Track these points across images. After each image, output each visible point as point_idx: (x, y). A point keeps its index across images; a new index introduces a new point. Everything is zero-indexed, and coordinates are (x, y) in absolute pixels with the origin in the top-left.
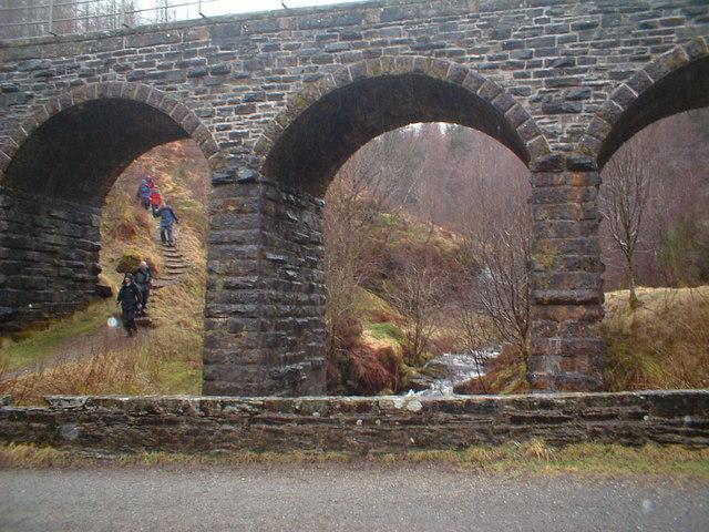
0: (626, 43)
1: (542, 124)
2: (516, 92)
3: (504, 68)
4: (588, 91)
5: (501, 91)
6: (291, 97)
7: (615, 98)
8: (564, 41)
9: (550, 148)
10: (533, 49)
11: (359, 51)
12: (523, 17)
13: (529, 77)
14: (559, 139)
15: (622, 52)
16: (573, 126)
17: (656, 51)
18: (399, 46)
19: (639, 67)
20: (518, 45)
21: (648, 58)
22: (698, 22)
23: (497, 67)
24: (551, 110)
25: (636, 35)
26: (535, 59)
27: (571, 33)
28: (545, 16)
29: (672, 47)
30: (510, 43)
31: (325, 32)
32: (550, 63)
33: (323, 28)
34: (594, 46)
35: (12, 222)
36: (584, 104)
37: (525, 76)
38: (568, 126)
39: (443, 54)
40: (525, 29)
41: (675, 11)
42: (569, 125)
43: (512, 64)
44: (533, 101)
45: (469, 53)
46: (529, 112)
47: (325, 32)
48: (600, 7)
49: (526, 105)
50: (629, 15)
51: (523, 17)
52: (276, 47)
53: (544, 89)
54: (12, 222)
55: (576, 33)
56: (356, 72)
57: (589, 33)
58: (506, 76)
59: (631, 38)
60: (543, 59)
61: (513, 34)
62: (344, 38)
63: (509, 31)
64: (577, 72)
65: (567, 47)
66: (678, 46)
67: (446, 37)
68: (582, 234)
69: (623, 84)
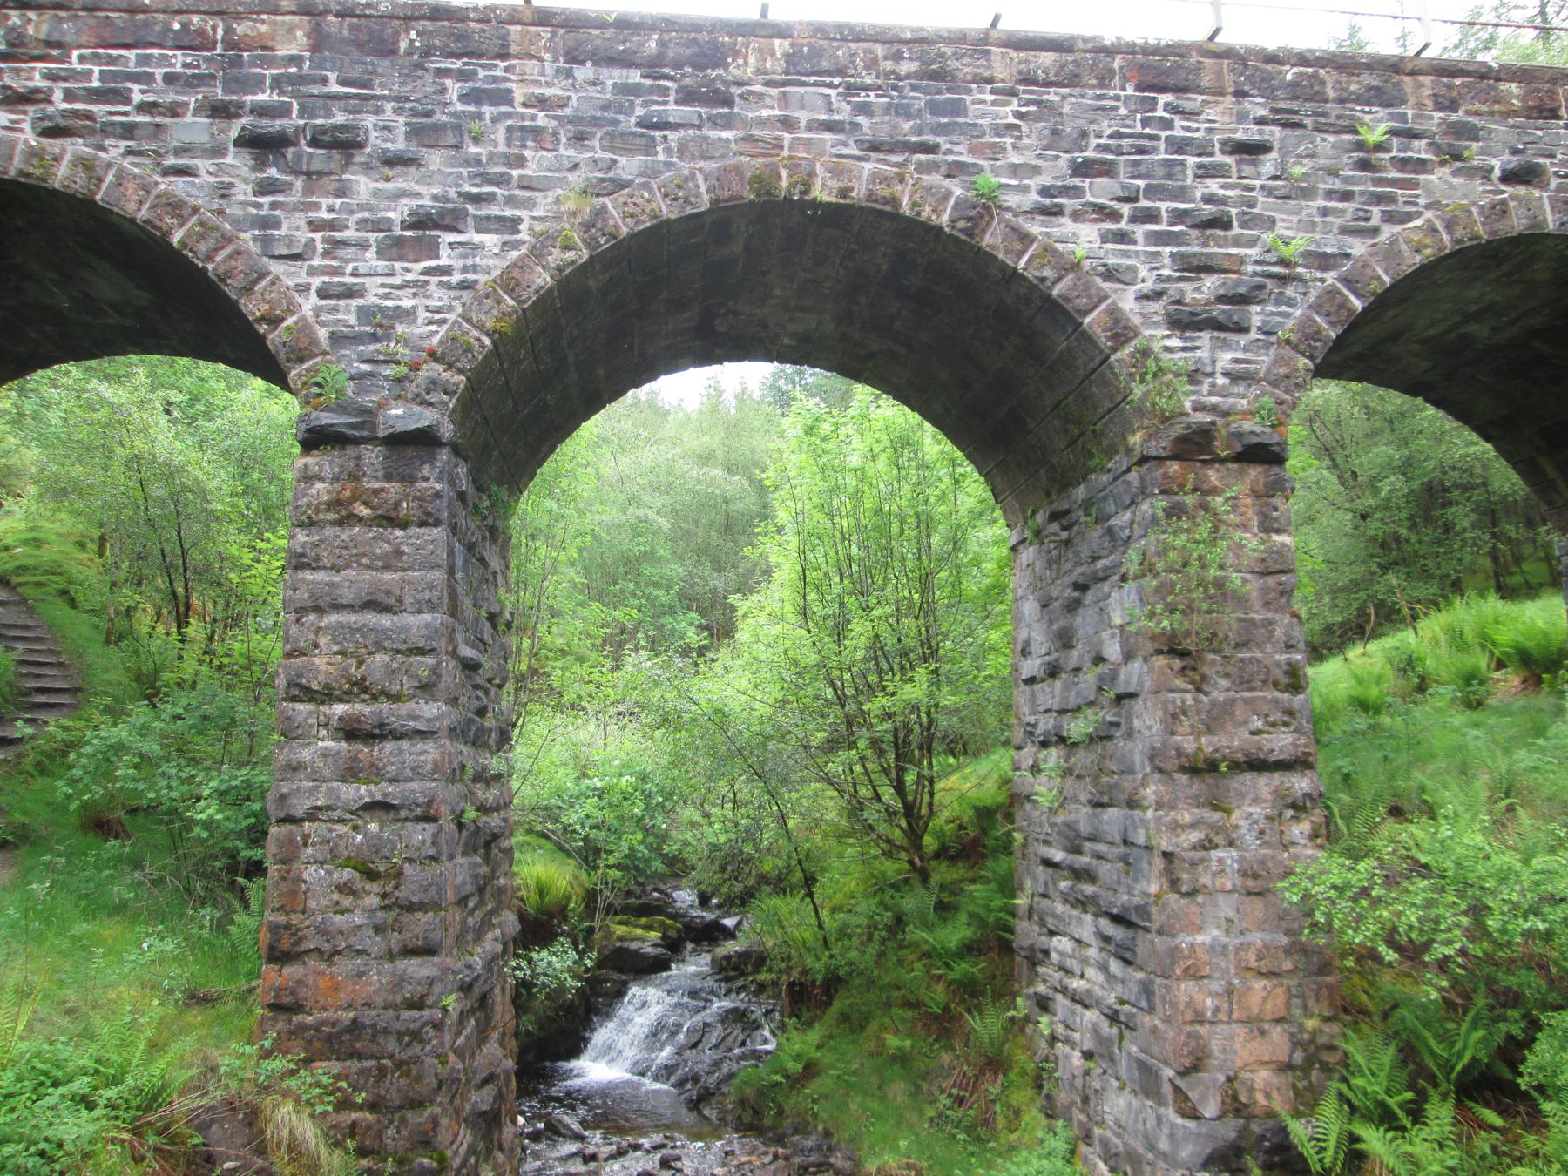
0: (1330, 194)
1: (1168, 349)
2: (1110, 274)
3: (1076, 216)
4: (1261, 287)
5: (1076, 266)
6: (538, 227)
7: (1316, 307)
8: (1205, 172)
9: (1188, 405)
10: (1141, 183)
11: (725, 134)
12: (1116, 108)
13: (1134, 242)
14: (1205, 388)
15: (1325, 212)
16: (1236, 361)
17: (1389, 218)
18: (827, 136)
19: (1358, 247)
20: (1107, 170)
21: (1375, 231)
22: (1456, 173)
23: (1056, 211)
24: (1185, 322)
25: (1347, 180)
26: (1144, 203)
27: (1219, 158)
28: (1160, 113)
29: (1419, 214)
30: (1088, 163)
31: (635, 76)
32: (1178, 216)
33: (631, 65)
34: (1269, 191)
35: (498, 354)
36: (1256, 314)
37: (1122, 237)
38: (1225, 358)
39: (932, 167)
40: (1119, 135)
41: (1416, 143)
42: (1228, 356)
43: (1099, 208)
44: (1144, 297)
45: (995, 172)
46: (1136, 320)
47: (635, 76)
48: (1275, 111)
49: (1127, 302)
50: (1331, 138)
51: (1116, 108)
52: (505, 97)
53: (1166, 272)
54: (498, 354)
55: (1230, 160)
56: (716, 181)
57: (1254, 163)
58: (1083, 239)
59: (1337, 185)
60: (1164, 206)
61: (1094, 142)
62: (687, 97)
63: (1084, 134)
64: (1237, 242)
65: (1213, 186)
66: (1429, 214)
67: (940, 130)
68: (1267, 604)
69: (1330, 277)
